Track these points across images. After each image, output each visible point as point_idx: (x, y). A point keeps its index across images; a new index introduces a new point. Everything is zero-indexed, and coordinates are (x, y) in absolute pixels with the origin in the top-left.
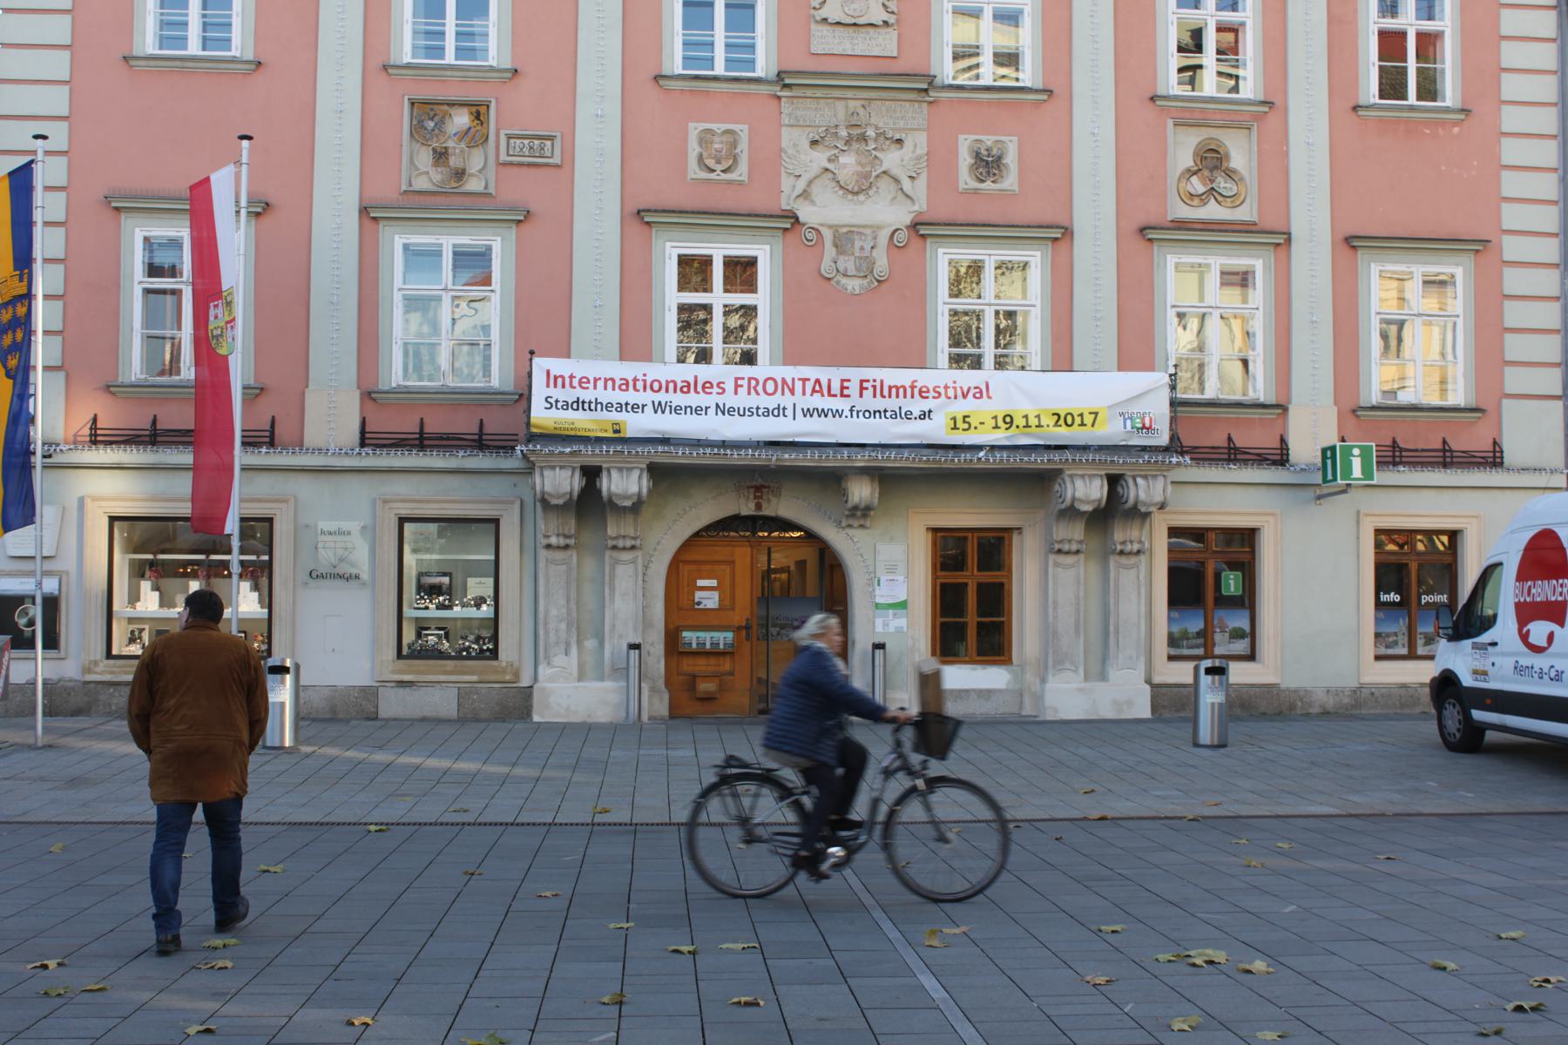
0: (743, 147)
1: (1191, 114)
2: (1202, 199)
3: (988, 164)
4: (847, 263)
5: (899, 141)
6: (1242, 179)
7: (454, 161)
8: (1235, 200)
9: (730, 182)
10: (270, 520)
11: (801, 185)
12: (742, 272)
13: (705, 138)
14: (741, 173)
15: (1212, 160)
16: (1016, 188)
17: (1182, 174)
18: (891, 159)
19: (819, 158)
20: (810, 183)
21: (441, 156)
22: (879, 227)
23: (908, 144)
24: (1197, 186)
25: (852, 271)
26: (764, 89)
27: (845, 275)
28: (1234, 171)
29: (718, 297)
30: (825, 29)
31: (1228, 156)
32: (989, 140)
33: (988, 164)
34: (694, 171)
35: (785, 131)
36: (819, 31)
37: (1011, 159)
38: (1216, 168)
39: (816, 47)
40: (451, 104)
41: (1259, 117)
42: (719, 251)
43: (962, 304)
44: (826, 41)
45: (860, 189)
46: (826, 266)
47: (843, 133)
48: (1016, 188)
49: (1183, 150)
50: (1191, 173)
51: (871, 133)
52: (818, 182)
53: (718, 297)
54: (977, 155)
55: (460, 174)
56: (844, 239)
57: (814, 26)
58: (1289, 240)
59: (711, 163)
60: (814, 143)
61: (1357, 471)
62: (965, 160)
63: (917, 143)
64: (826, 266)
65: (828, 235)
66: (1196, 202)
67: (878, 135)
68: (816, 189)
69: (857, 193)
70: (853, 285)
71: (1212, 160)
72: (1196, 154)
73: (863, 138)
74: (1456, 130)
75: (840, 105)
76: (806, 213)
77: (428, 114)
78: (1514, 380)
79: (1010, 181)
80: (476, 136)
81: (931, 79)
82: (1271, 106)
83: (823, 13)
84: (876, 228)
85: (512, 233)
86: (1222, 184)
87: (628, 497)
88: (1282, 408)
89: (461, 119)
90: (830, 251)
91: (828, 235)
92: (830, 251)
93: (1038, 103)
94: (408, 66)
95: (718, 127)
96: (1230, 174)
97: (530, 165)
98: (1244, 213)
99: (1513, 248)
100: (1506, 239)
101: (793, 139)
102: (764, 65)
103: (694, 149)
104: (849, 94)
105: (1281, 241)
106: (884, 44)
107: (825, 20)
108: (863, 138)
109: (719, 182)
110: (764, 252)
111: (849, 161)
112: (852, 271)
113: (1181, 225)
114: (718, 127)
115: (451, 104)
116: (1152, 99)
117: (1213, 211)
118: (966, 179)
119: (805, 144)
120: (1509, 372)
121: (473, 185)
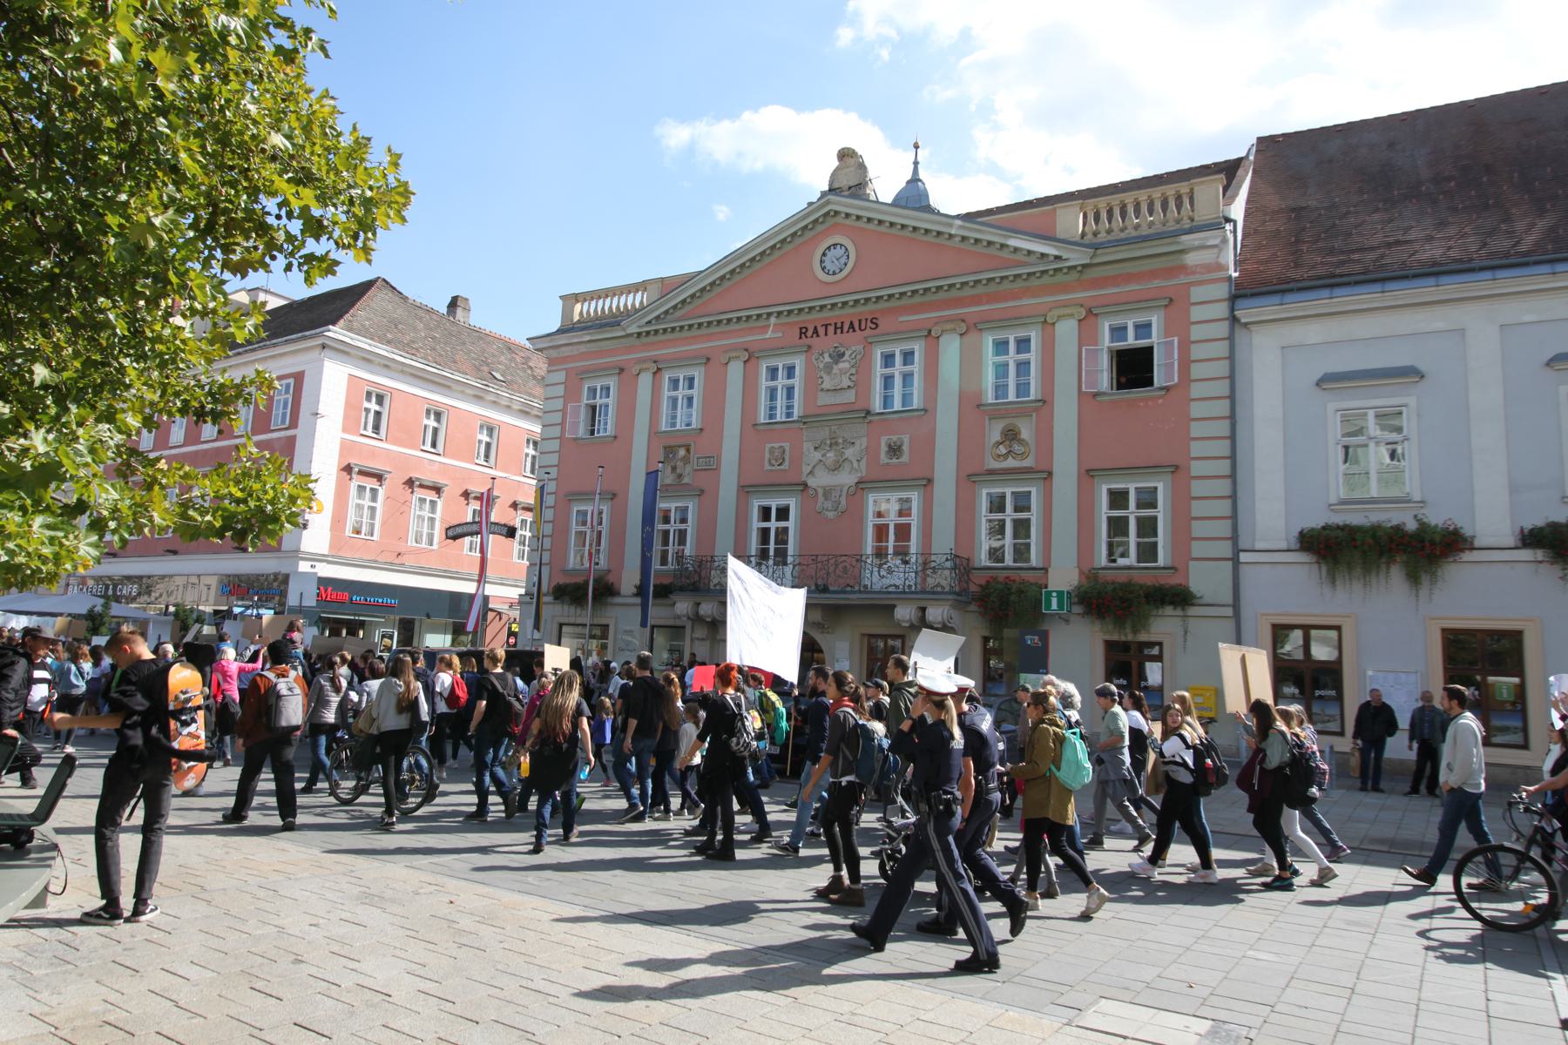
0: (787, 453)
1: (996, 412)
2: (1006, 456)
3: (895, 450)
4: (829, 505)
5: (853, 443)
6: (1027, 444)
7: (678, 471)
8: (1023, 456)
9: (781, 470)
10: (608, 626)
11: (810, 468)
12: (783, 513)
13: (772, 451)
14: (785, 466)
15: (1011, 435)
16: (907, 461)
17: (994, 445)
18: (850, 453)
19: (818, 455)
20: (814, 467)
21: (674, 469)
22: (843, 486)
23: (858, 443)
24: (1003, 450)
25: (830, 508)
26: (796, 425)
27: (827, 510)
28: (1023, 440)
29: (773, 524)
30: (823, 394)
31: (1019, 433)
32: (895, 438)
33: (895, 450)
34: (767, 467)
35: (805, 444)
36: (821, 395)
37: (905, 448)
38: (1013, 439)
39: (819, 403)
40: (679, 446)
41: (1036, 409)
42: (774, 504)
43: (999, 516)
44: (824, 399)
45: (836, 468)
46: (819, 507)
47: (828, 442)
48: (907, 461)
49: (995, 434)
50: (999, 444)
51: (840, 441)
52: (817, 467)
53: (773, 524)
54: (890, 446)
55: (680, 476)
56: (827, 492)
57: (819, 393)
58: (1050, 474)
59: (773, 462)
60: (816, 448)
61: (1054, 606)
62: (884, 448)
63: (862, 443)
64: (819, 507)
65: (820, 492)
66: (1002, 458)
67: (844, 441)
68: (816, 471)
69: (834, 470)
70: (831, 515)
71: (1011, 435)
72: (1002, 433)
73: (837, 444)
74: (1160, 401)
75: (827, 429)
76: (811, 482)
77: (670, 450)
78: (1198, 549)
79: (905, 458)
80: (686, 460)
81: (868, 413)
82: (1045, 402)
83: (823, 386)
84: (842, 486)
85: (696, 500)
86: (1017, 448)
87: (709, 617)
88: (1045, 570)
89: (682, 452)
90: (821, 498)
91: (820, 492)
92: (821, 498)
93: (919, 417)
94: (665, 432)
95: (776, 445)
96: (1022, 442)
97: (705, 470)
98: (1028, 463)
99: (1197, 468)
100: (1193, 463)
101: (808, 446)
102: (796, 413)
103: (767, 455)
104: (830, 423)
105: (1046, 476)
106: (850, 397)
107: (822, 390)
108: (837, 444)
109: (776, 471)
110: (792, 503)
111: (831, 455)
112: (830, 508)
113: (991, 472)
114: (776, 445)
115: (679, 446)
116: (978, 406)
117: (1011, 463)
118: (884, 458)
119: (812, 448)
120: (1194, 544)
121: (686, 480)
